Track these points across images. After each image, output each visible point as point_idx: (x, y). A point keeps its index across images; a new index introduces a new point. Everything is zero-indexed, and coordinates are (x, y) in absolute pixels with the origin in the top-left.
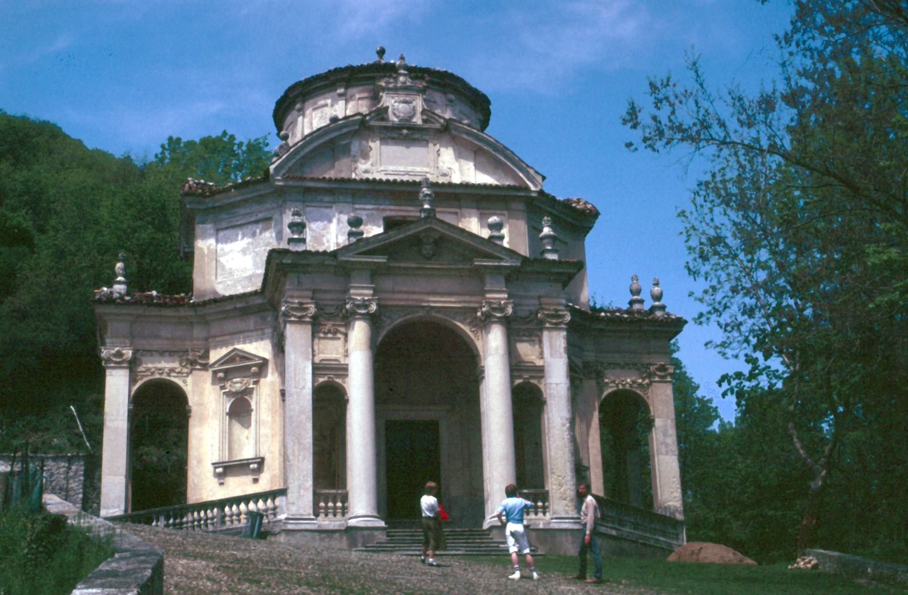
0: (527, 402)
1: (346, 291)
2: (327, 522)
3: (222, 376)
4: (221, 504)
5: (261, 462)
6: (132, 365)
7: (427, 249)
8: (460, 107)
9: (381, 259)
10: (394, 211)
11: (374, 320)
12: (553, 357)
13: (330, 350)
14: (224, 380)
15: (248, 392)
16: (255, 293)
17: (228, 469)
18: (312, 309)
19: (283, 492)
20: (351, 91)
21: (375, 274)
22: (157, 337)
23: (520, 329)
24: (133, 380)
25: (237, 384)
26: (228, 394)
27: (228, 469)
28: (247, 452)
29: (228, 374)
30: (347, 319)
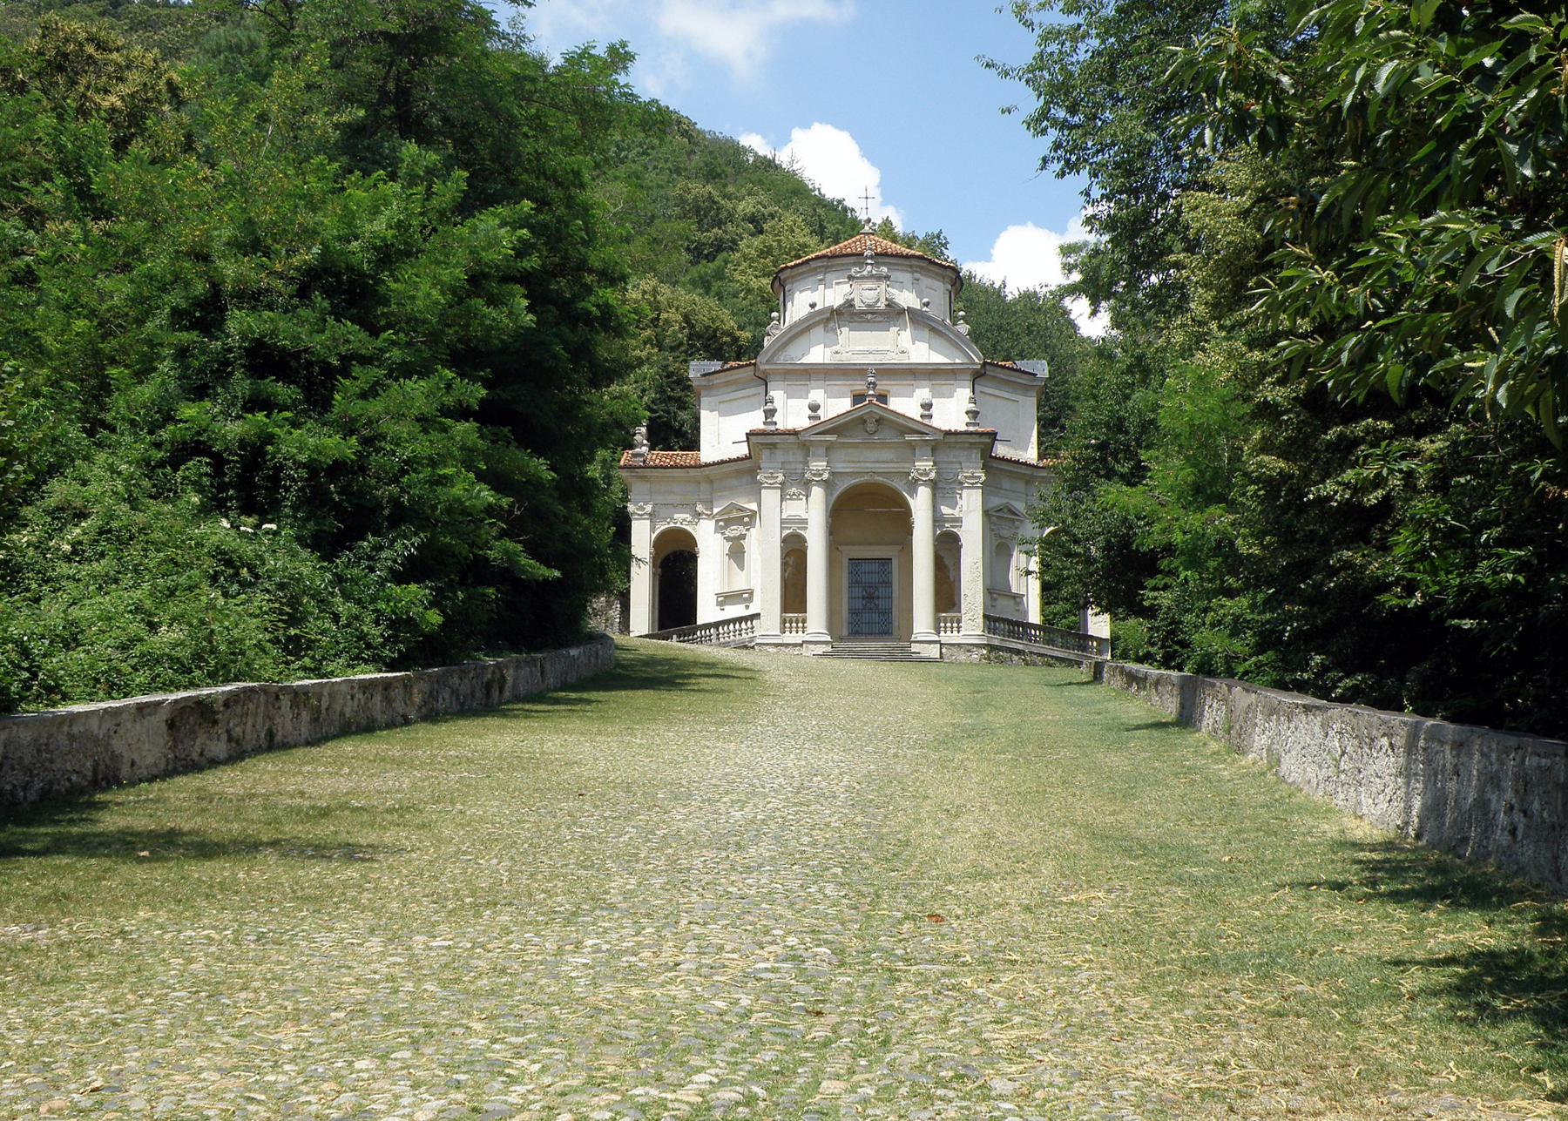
0: (947, 546)
1: (806, 463)
2: (789, 638)
3: (724, 523)
4: (717, 625)
5: (751, 594)
6: (652, 517)
7: (871, 427)
8: (926, 281)
9: (833, 438)
10: (860, 386)
11: (827, 485)
12: (969, 511)
13: (795, 508)
14: (726, 527)
15: (743, 537)
16: (746, 458)
17: (727, 599)
18: (781, 478)
19: (757, 616)
20: (828, 276)
21: (829, 448)
22: (671, 492)
23: (942, 489)
24: (653, 529)
25: (734, 531)
26: (728, 539)
27: (727, 599)
28: (739, 584)
29: (729, 522)
30: (806, 485)
